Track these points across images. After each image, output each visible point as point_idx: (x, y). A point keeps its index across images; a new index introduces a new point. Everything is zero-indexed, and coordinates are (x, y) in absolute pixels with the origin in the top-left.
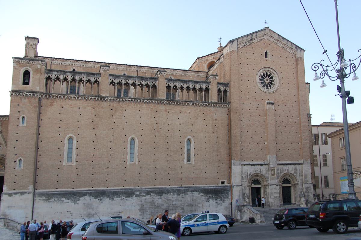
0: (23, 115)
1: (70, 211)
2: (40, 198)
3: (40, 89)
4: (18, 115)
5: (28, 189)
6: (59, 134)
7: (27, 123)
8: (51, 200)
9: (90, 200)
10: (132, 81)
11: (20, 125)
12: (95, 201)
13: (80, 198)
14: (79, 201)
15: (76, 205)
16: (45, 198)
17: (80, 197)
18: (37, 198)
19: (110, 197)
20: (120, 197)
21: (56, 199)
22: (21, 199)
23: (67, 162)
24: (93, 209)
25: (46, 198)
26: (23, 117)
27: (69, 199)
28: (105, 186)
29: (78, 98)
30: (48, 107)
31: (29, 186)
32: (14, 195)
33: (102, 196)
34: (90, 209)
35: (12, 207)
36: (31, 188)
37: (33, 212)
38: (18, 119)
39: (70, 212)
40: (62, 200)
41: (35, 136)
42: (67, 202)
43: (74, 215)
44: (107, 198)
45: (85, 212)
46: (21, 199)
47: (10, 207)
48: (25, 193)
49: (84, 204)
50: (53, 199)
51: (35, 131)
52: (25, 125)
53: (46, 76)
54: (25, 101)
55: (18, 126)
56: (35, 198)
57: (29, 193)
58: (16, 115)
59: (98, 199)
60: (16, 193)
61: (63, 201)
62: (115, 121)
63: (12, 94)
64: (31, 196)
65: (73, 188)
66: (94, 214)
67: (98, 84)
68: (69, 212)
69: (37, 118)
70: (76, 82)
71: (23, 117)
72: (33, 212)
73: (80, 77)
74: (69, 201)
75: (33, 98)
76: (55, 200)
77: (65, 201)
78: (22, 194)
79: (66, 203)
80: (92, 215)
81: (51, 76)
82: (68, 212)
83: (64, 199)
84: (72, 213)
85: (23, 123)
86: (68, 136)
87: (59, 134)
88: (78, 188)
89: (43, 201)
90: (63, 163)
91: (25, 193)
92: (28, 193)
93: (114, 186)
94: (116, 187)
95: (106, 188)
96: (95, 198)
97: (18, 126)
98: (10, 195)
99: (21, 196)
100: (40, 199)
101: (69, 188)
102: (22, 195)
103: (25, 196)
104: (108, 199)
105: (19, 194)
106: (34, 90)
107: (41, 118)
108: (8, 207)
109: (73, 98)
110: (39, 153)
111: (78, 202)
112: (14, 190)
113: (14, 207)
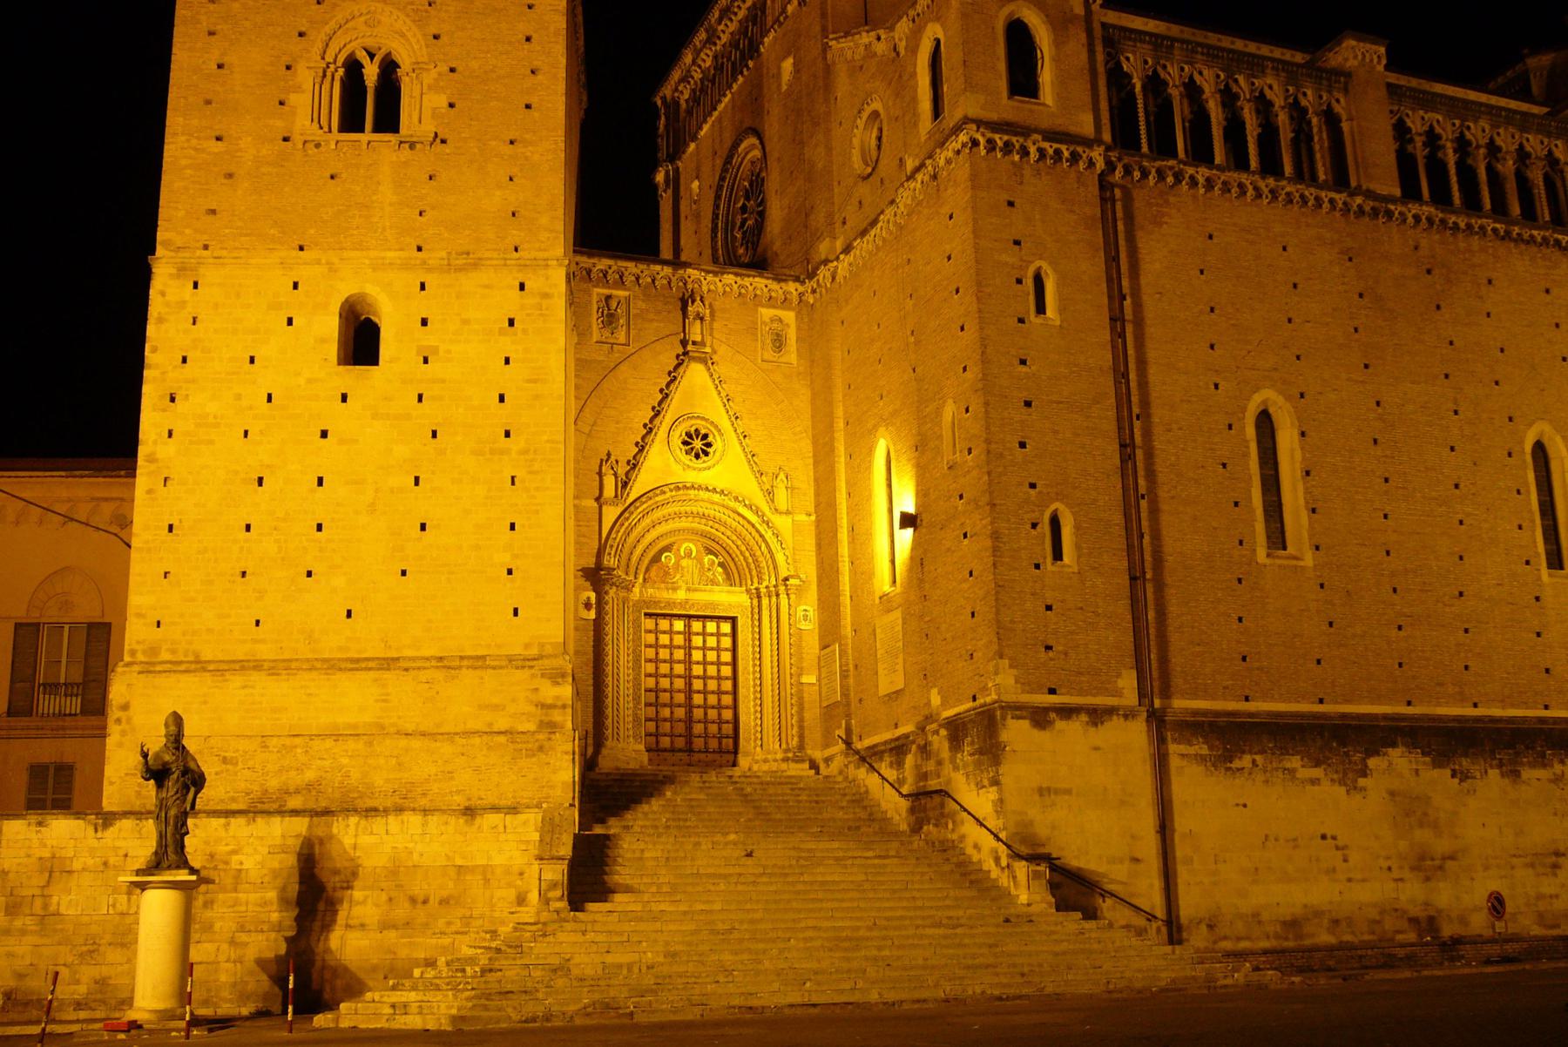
0: (1038, 263)
1: (1334, 833)
2: (1183, 748)
5: (1118, 693)
8: (1237, 764)
9: (1417, 771)
12: (1437, 782)
13: (1372, 762)
14: (1365, 775)
15: (1358, 797)
16: (1204, 750)
18: (1173, 748)
19: (1500, 766)
20: (1544, 766)
22: (1096, 749)
24: (1435, 826)
25: (1211, 748)
27: (1317, 765)
28: (1461, 699)
31: (1119, 675)
32: (1060, 724)
33: (1466, 755)
34: (1421, 825)
39: (1334, 838)
40: (1288, 765)
42: (1315, 782)
43: (1354, 857)
44: (1492, 767)
45: (1403, 845)
46: (1096, 749)
47: (1049, 789)
48: (1110, 711)
49: (1392, 794)
50: (1245, 762)
57: (1129, 715)
59: (1448, 772)
60: (1067, 712)
61: (1292, 771)
64: (1136, 734)
65: (1321, 701)
66: (1444, 859)
68: (1329, 841)
74: (1317, 772)
76: (1254, 761)
78: (1097, 715)
79: (1309, 787)
80: (1437, 863)
82: (1324, 837)
83: (1294, 762)
84: (1344, 848)
88: (1348, 701)
89: (1202, 768)
91: (1110, 711)
92: (1126, 717)
93: (1504, 702)
94: (1513, 706)
95: (1470, 711)
96: (1437, 764)
98: (1040, 718)
99: (1092, 730)
100: (1183, 755)
101: (1301, 697)
102: (1095, 725)
104: (1494, 773)
105: (1084, 717)
108: (1041, 791)
111: (1362, 782)
112: (1052, 691)
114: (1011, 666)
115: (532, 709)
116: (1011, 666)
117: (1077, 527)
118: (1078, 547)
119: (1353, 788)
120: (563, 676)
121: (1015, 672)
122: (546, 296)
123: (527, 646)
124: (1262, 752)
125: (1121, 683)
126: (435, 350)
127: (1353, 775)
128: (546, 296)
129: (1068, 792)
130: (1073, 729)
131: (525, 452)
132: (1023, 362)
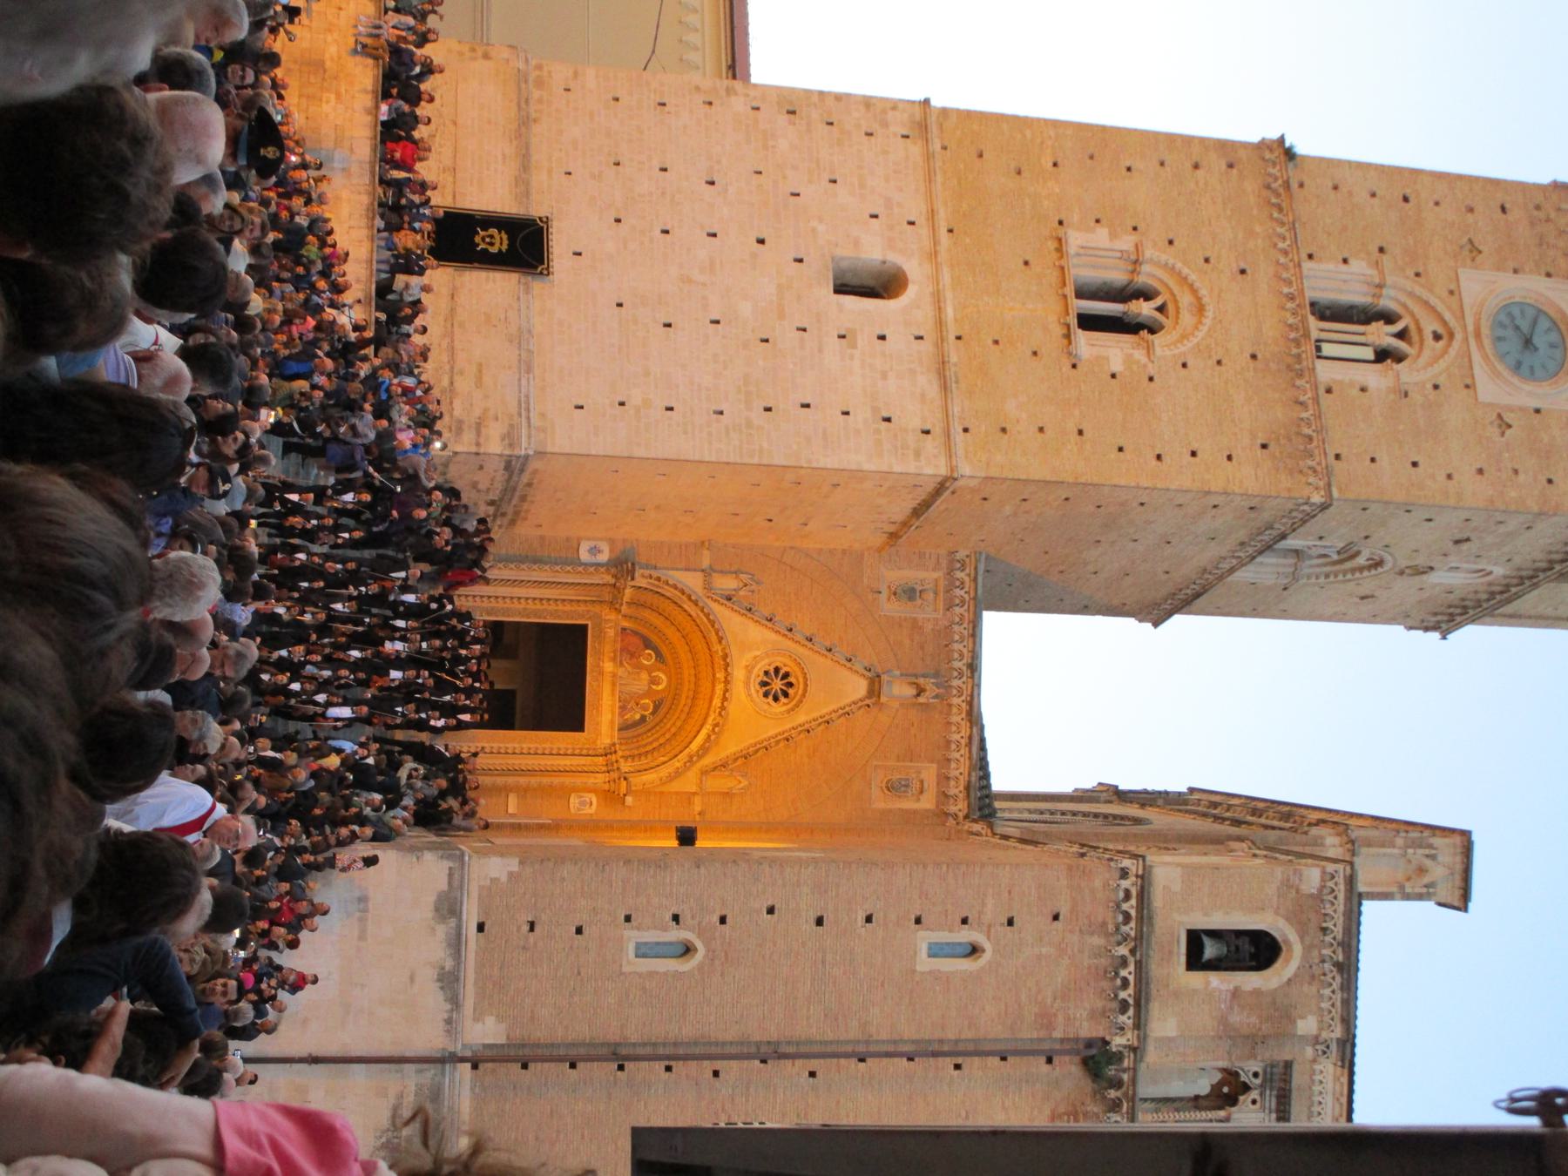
4: (988, 917)
7: (936, 975)
11: (922, 934)
22: (412, 979)
26: (974, 950)
31: (500, 1018)
32: (442, 931)
35: (362, 920)
36: (485, 1031)
37: (314, 1060)
38: (964, 921)
41: (851, 1031)
46: (412, 979)
47: (365, 911)
48: (455, 1002)
51: (882, 1032)
52: (924, 963)
55: (918, 921)
56: (410, 1068)
58: (990, 902)
60: (456, 943)
64: (428, 1038)
69: (968, 1034)
71: (974, 950)
72: (314, 1060)
78: (449, 981)
85: (936, 951)
91: (455, 1002)
92: (449, 1021)
97: (918, 921)
98: (448, 907)
103: (433, 1001)
105: (449, 964)
107: (973, 1065)
110: (730, 1069)
112: (481, 928)
113: (362, 936)
114: (511, 874)
115: (477, 412)
116: (511, 874)
117: (678, 975)
118: (652, 974)
120: (511, 445)
121: (504, 879)
122: (918, 454)
123: (543, 415)
125: (490, 1021)
126: (854, 346)
128: (918, 454)
129: (362, 936)
130: (435, 950)
131: (749, 424)
132: (869, 919)
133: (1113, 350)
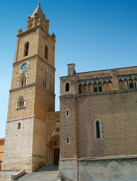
3: (75, 93)
6: (90, 120)
10: (134, 77)
13: (108, 163)
14: (107, 165)
17: (108, 162)
21: (92, 164)
23: (96, 137)
27: (100, 164)
29: (99, 94)
30: (81, 103)
39: (102, 173)
42: (99, 166)
43: (105, 175)
50: (90, 164)
53: (78, 84)
54: (68, 101)
61: (96, 165)
62: (126, 106)
63: (60, 98)
67: (111, 83)
68: (101, 173)
70: (97, 84)
73: (99, 81)
74: (100, 165)
75: (72, 99)
76: (91, 165)
77: (98, 165)
81: (81, 84)
82: (101, 173)
84: (104, 174)
86: (96, 120)
87: (90, 120)
90: (94, 139)
106: (72, 94)
109: (96, 95)
111: (107, 166)
119: (105, 167)
124: (92, 163)
127: (105, 166)
133: (25, 103)
